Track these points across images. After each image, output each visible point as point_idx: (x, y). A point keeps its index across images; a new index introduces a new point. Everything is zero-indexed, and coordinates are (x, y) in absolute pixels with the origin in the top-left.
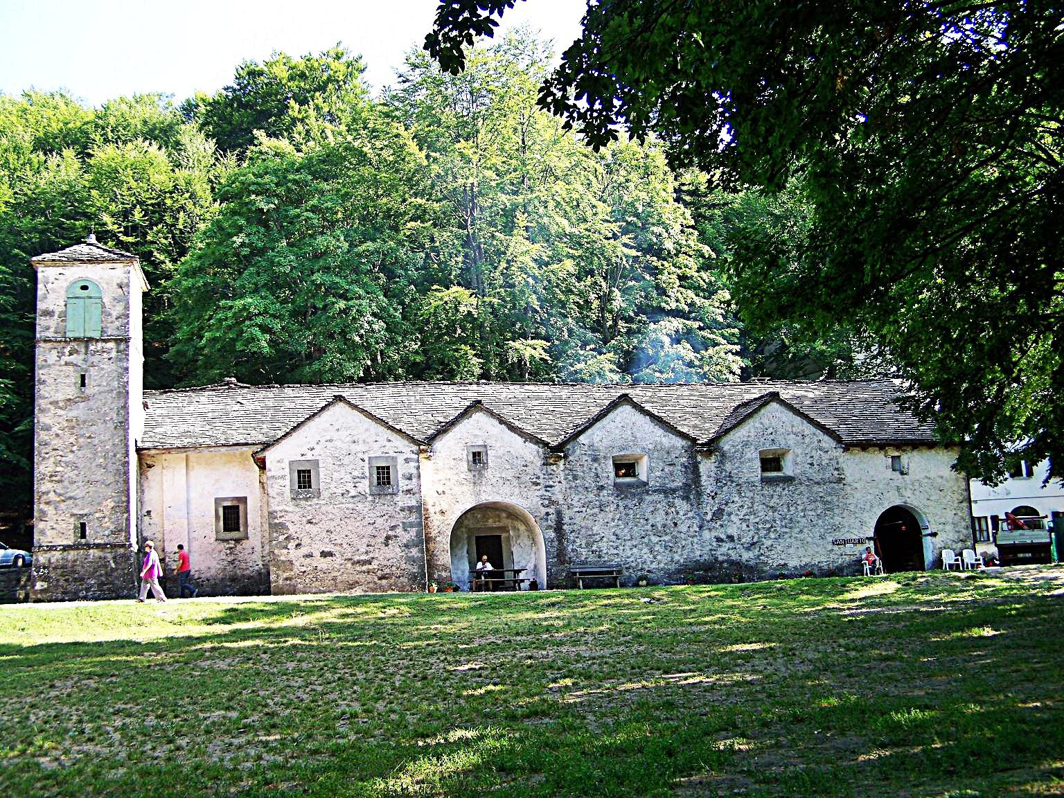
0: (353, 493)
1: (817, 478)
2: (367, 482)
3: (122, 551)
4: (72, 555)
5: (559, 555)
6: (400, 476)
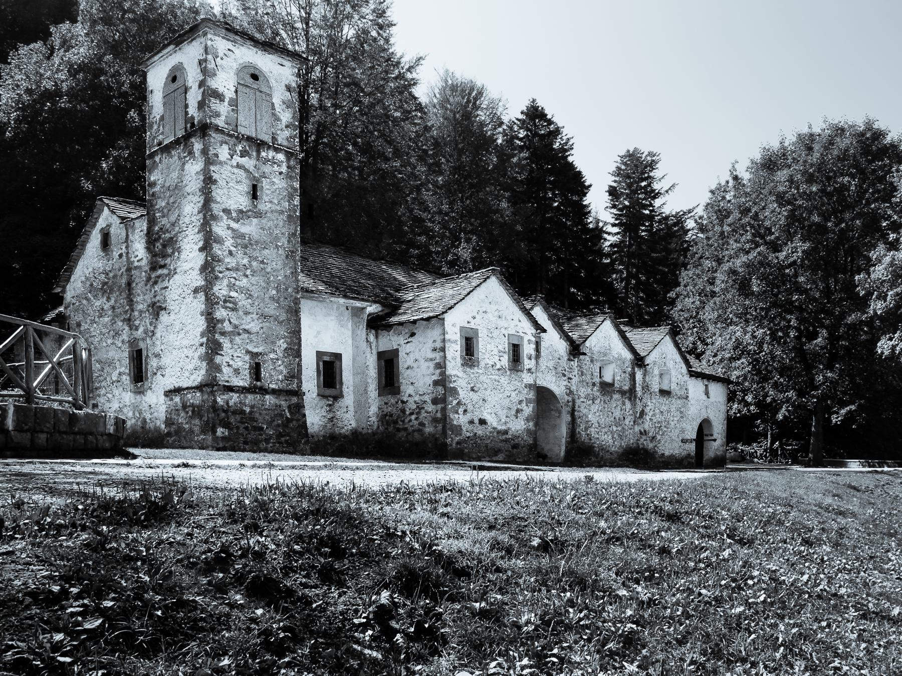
0: (498, 367)
1: (679, 393)
2: (506, 357)
3: (295, 400)
4: (250, 398)
5: (573, 433)
6: (525, 355)
